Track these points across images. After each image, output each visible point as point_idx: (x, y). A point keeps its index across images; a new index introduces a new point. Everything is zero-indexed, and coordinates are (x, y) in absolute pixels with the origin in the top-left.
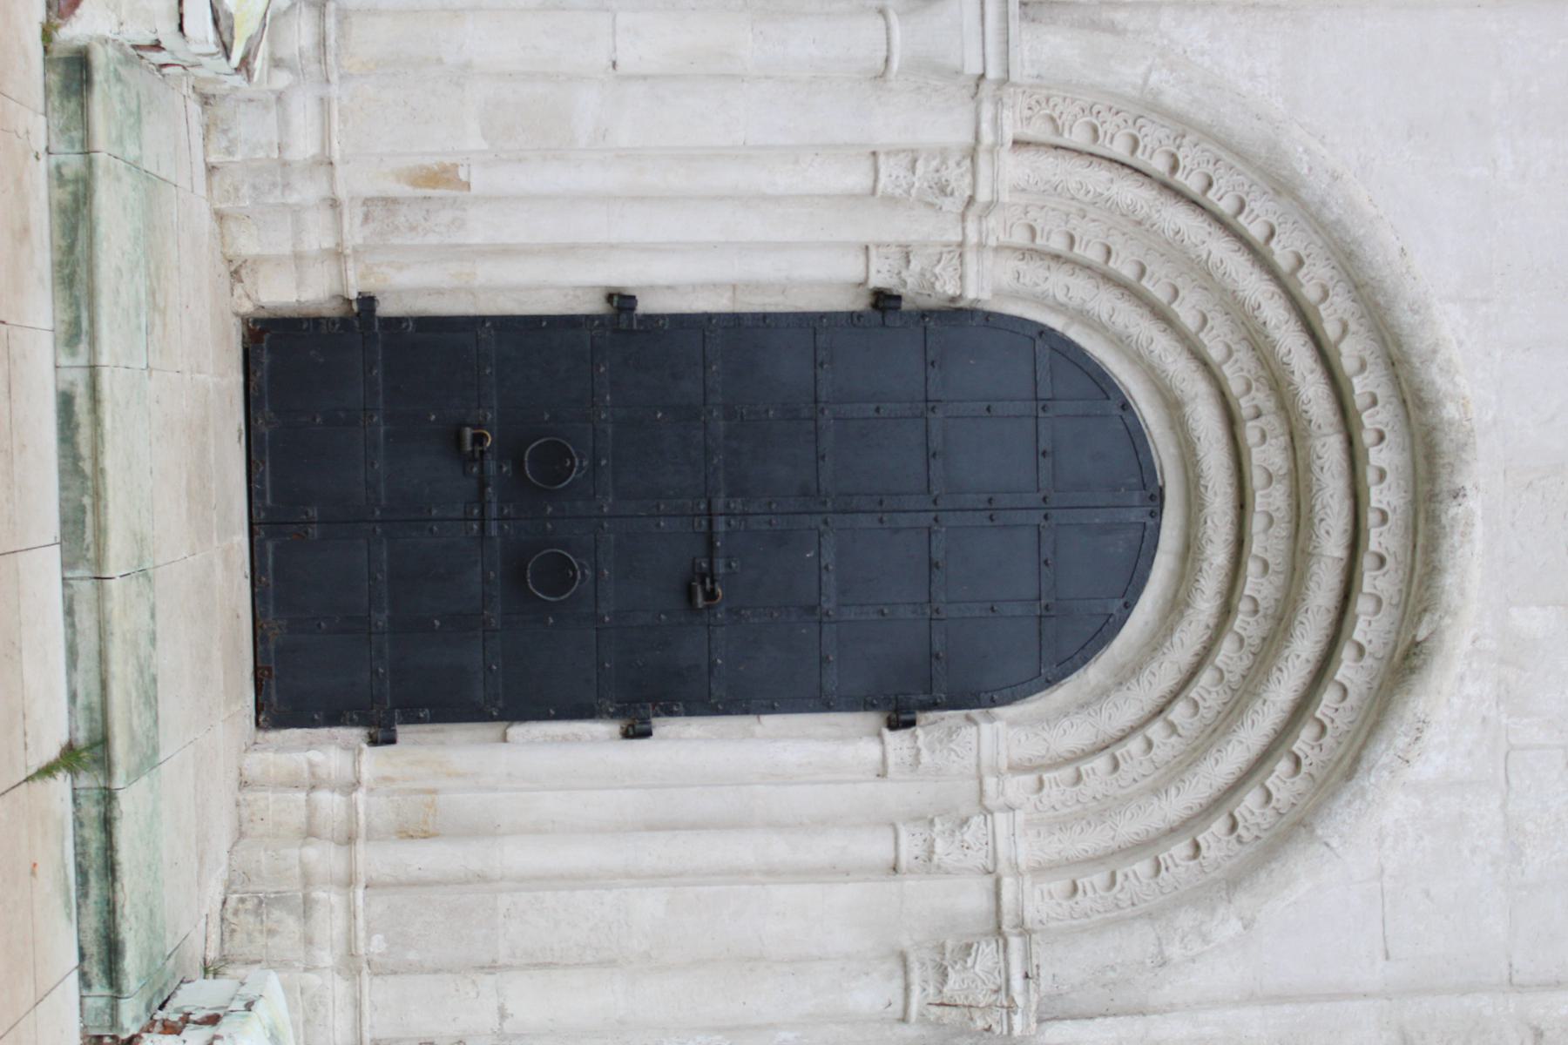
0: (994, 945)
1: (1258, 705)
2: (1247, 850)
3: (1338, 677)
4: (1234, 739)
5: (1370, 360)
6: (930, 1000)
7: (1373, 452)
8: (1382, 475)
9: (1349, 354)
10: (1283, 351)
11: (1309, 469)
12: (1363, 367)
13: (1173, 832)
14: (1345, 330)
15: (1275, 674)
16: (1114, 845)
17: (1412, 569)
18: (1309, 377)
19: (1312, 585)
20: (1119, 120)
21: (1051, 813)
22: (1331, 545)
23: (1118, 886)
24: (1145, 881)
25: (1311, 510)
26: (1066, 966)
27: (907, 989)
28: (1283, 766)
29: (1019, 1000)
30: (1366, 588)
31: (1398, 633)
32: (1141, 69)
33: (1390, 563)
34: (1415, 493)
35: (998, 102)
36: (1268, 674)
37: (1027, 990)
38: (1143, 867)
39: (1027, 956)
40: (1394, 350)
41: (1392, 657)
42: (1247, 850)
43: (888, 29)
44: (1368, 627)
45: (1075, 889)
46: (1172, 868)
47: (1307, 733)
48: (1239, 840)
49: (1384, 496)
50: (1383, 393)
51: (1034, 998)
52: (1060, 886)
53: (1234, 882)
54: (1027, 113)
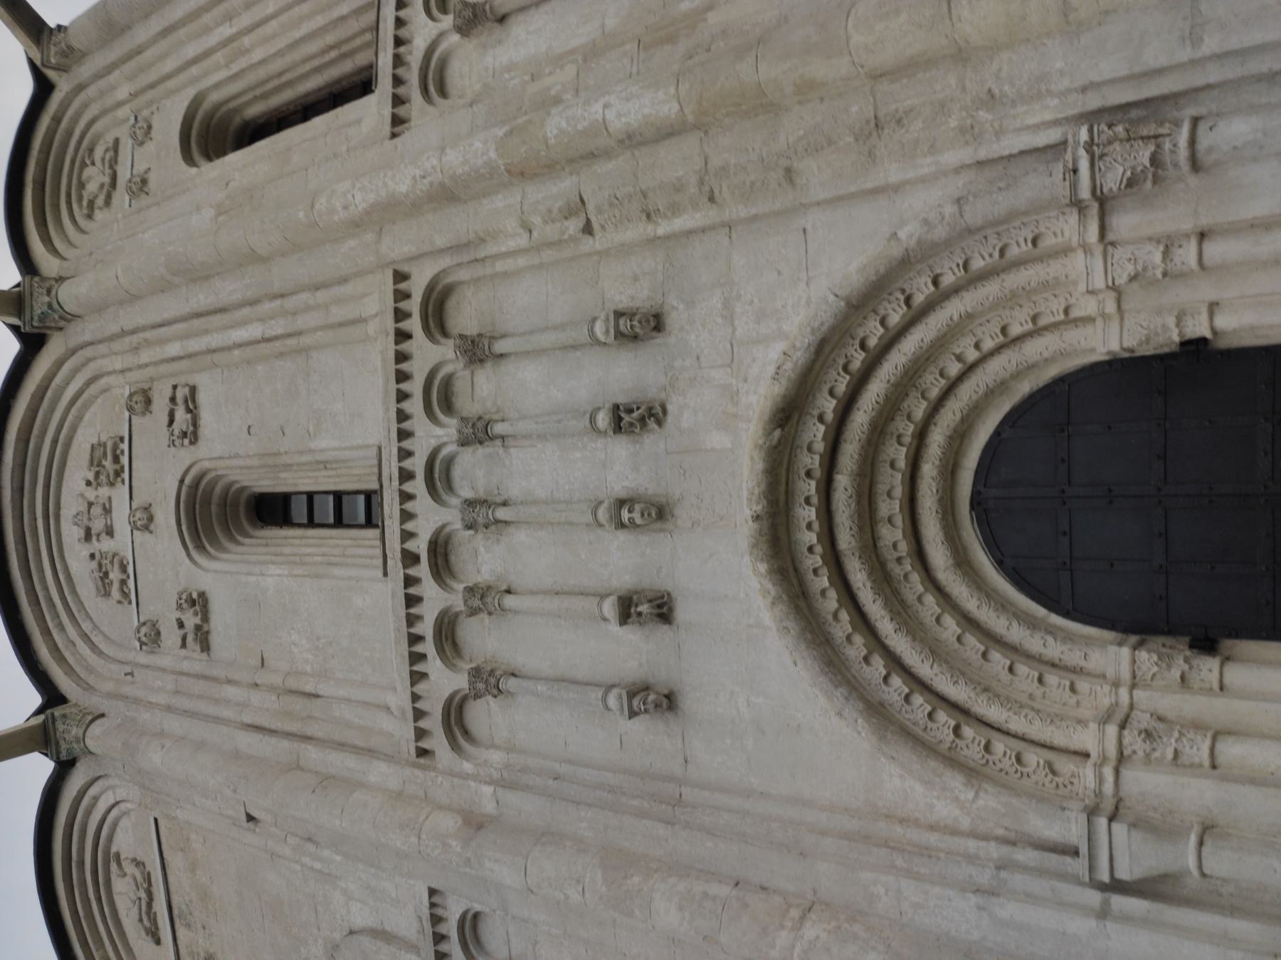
0: (1105, 190)
1: (893, 379)
2: (898, 285)
3: (834, 402)
4: (910, 355)
5: (818, 596)
6: (1167, 139)
7: (815, 540)
8: (809, 526)
9: (831, 602)
10: (878, 603)
11: (861, 528)
12: (823, 592)
13: (956, 290)
14: (835, 616)
15: (881, 400)
16: (1003, 276)
17: (788, 470)
18: (861, 585)
19: (856, 456)
20: (999, 766)
21: (1057, 292)
22: (843, 481)
23: (997, 249)
24: (976, 255)
25: (858, 503)
26: (1045, 183)
27: (1192, 142)
28: (872, 342)
29: (1082, 153)
30: (817, 458)
31: (796, 431)
32: (981, 803)
33: (802, 474)
34: (787, 516)
35: (1099, 794)
36: (887, 398)
37: (1075, 161)
38: (978, 264)
39: (1074, 187)
40: (802, 603)
41: (800, 417)
42: (898, 285)
43: (1200, 867)
44: (816, 433)
45: (1035, 242)
46: (954, 267)
47: (856, 365)
48: (903, 291)
49: (809, 514)
50: (810, 576)
51: (1069, 156)
52: (1048, 242)
53: (905, 263)
54: (1075, 781)
